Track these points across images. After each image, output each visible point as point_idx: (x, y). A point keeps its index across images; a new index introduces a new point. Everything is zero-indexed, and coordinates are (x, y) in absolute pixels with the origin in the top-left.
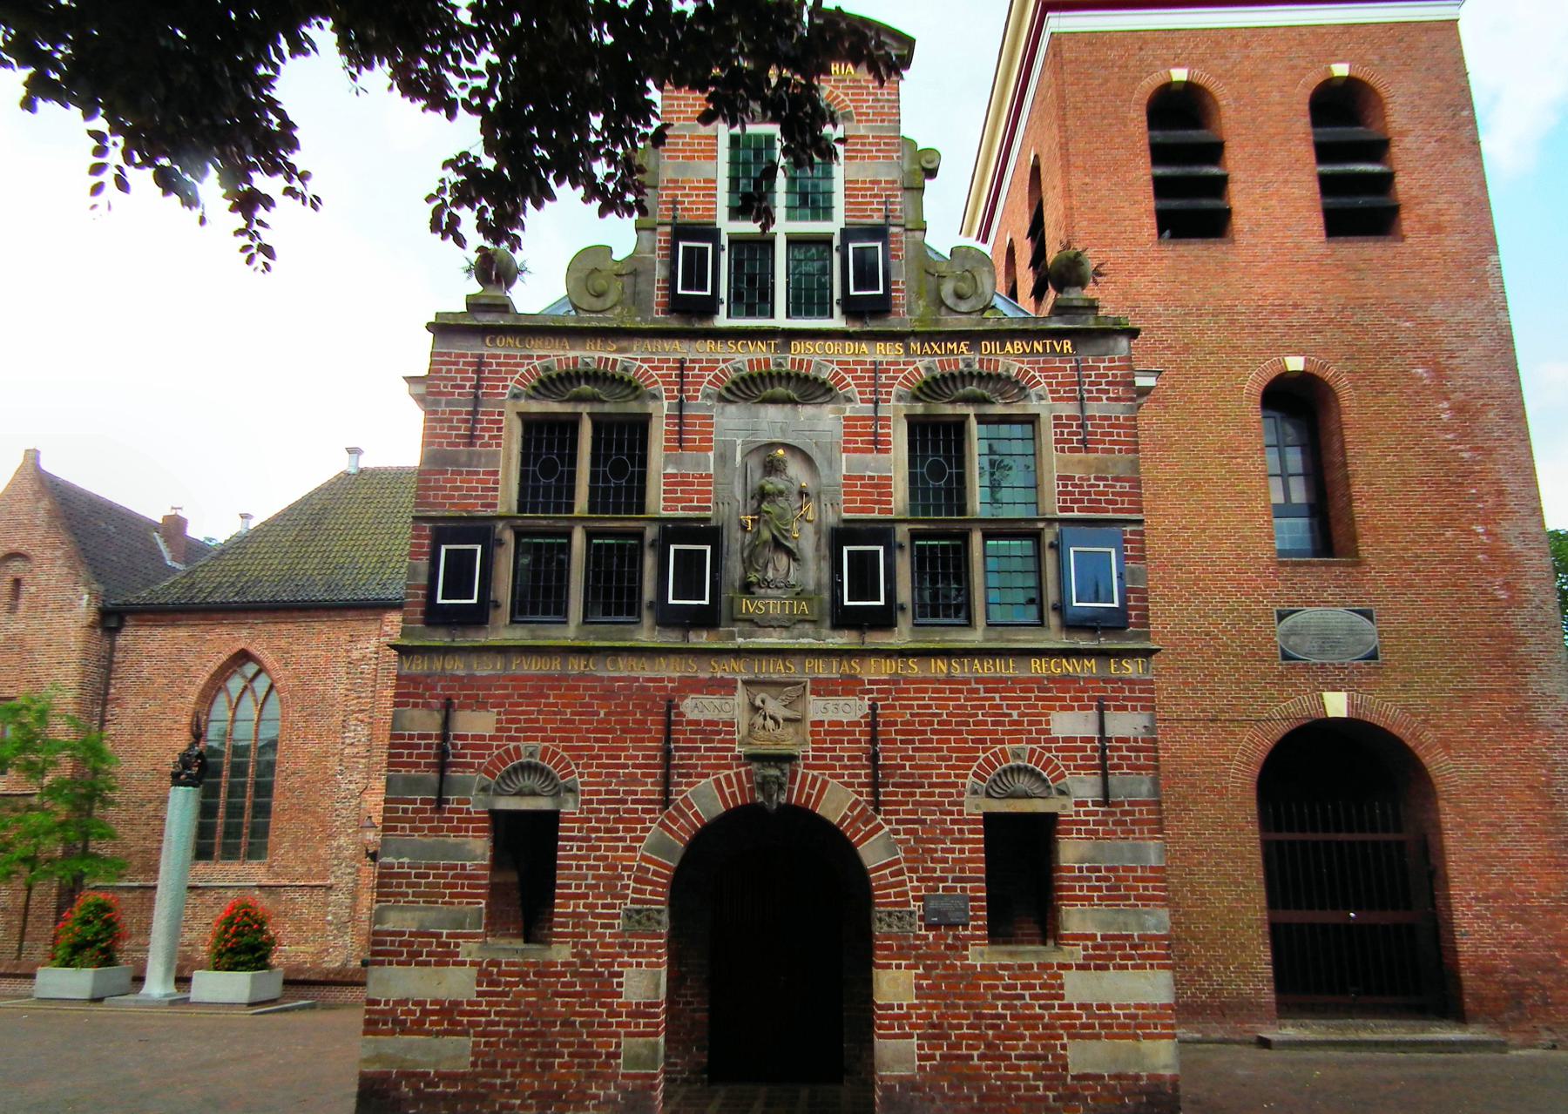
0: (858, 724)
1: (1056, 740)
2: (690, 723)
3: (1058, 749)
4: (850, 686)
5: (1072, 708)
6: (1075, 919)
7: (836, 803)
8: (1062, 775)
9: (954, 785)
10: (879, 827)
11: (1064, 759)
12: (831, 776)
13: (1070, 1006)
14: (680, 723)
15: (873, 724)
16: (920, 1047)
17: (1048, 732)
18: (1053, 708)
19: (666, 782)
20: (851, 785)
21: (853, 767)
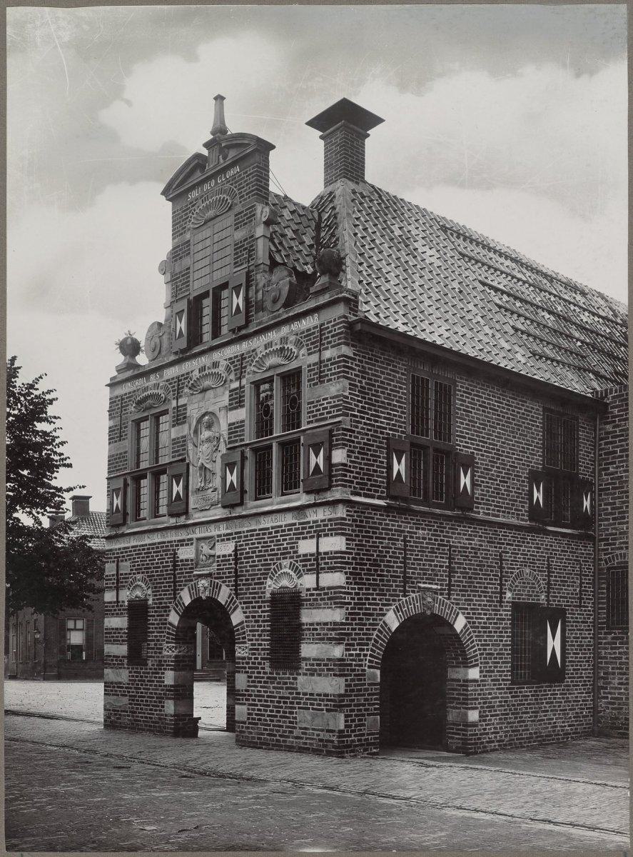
0: (230, 555)
1: (300, 556)
2: (182, 561)
3: (301, 561)
4: (227, 537)
5: (306, 538)
6: (309, 650)
7: (223, 596)
8: (301, 576)
9: (262, 583)
10: (237, 607)
11: (304, 566)
12: (223, 582)
13: (299, 694)
14: (178, 561)
15: (236, 555)
16: (248, 709)
17: (296, 552)
18: (299, 539)
19: (175, 590)
20: (228, 586)
21: (229, 577)
